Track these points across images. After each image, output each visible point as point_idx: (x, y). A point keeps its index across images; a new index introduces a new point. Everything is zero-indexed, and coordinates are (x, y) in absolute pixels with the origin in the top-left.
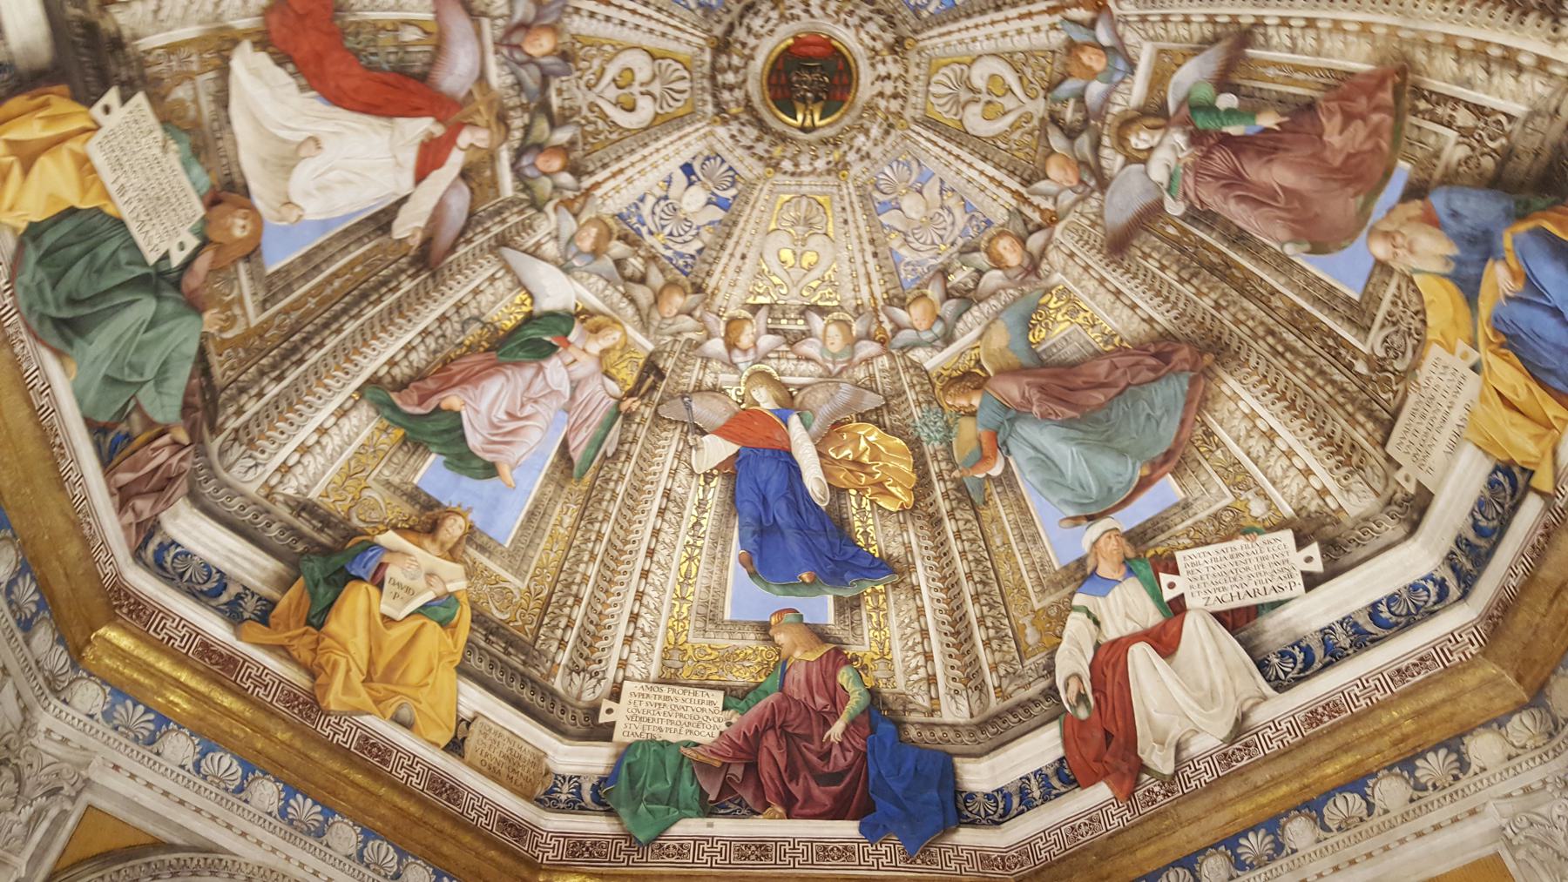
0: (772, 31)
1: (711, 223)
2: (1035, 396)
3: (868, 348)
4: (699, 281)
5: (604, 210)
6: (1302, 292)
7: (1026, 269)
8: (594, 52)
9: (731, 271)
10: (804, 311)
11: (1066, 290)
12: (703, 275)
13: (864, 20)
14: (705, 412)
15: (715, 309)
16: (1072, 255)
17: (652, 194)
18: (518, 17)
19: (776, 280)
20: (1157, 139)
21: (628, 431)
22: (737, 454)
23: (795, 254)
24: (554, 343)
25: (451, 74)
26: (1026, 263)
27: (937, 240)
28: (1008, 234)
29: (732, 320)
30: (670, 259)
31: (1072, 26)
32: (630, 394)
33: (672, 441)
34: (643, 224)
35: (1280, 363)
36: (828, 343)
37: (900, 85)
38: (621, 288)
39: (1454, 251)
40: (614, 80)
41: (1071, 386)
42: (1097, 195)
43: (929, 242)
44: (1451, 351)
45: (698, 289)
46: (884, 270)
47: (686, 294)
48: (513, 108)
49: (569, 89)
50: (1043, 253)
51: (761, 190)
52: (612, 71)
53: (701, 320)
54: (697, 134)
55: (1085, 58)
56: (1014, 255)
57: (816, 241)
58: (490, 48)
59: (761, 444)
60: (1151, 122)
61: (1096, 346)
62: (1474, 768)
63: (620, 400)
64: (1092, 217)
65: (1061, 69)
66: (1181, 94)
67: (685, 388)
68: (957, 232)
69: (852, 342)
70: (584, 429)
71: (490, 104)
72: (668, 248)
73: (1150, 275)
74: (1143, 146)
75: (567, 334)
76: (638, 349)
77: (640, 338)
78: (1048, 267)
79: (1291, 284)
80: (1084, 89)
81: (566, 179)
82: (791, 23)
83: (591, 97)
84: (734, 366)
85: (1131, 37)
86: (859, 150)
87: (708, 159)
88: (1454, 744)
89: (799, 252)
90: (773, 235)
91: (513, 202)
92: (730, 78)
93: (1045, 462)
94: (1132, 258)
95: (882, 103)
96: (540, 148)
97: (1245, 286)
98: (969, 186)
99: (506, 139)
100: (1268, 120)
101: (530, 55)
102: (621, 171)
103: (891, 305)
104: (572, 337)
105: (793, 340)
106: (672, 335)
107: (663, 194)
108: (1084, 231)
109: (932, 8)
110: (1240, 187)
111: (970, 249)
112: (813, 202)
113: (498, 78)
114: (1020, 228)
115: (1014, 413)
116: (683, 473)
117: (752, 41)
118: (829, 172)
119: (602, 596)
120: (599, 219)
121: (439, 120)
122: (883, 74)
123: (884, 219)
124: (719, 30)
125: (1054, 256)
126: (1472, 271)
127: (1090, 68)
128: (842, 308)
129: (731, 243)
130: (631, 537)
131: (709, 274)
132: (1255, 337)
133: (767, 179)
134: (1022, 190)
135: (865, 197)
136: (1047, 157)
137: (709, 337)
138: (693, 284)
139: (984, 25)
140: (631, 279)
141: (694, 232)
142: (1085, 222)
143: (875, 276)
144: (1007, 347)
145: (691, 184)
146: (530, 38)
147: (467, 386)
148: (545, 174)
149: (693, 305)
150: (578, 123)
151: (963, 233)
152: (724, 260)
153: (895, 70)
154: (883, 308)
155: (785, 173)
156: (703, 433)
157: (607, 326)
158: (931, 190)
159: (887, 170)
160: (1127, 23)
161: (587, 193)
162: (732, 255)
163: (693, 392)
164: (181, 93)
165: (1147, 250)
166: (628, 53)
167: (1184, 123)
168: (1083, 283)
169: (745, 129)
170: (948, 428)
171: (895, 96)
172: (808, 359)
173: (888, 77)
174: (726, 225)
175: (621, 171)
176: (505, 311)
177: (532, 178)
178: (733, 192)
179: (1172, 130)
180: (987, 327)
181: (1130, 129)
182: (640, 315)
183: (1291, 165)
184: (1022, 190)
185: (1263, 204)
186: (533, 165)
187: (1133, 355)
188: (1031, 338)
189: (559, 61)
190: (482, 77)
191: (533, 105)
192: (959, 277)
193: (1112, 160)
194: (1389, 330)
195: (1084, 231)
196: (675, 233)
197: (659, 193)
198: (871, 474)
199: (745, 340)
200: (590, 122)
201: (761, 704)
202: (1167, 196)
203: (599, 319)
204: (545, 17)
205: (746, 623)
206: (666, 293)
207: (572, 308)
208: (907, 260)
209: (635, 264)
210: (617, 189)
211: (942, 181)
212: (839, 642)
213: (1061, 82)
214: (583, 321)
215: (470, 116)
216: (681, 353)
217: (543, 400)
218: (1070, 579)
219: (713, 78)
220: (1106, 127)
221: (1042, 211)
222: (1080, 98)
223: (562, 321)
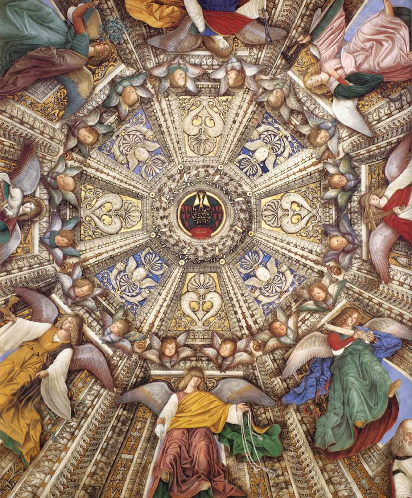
0: (222, 238)
1: (254, 140)
3: (160, 72)
4: (260, 109)
5: (311, 151)
7: (75, 128)
8: (311, 234)
9: (241, 113)
10: (198, 93)
11: (52, 120)
12: (257, 112)
13: (176, 245)
15: (250, 93)
16: (52, 138)
17: (285, 158)
18: (348, 257)
19: (215, 109)
20: (21, 209)
21: (307, 22)
23: (205, 124)
24: (347, 82)
25: (385, 236)
26: (76, 131)
27: (127, 137)
28: (88, 145)
29: (241, 87)
30: (276, 122)
31: (75, 254)
34: (290, 142)
36: (183, 75)
37: (155, 214)
38: (305, 108)
40: (302, 219)
41: (38, 69)
42: (46, 173)
43: (131, 136)
45: (260, 104)
46: (154, 118)
47: (267, 101)
48: (355, 212)
49: (326, 217)
50: (67, 137)
51: (225, 158)
52: (302, 224)
53: (259, 86)
54: (260, 187)
55: (65, 240)
56: (83, 134)
57: (195, 131)
58: (364, 244)
60: (26, 217)
61: (27, 93)
64: (45, 161)
65: (76, 233)
66: (15, 234)
67: (270, 46)
68: (117, 143)
69: (170, 75)
70: (334, 28)
71: (367, 218)
72: (278, 129)
73: (7, 136)
74: (28, 205)
75: (338, 86)
76: (297, 73)
77: (295, 78)
78: (63, 130)
80: (63, 226)
81: (331, 170)
82: (212, 242)
83: (314, 212)
84: (240, 60)
85: (45, 255)
86: (174, 180)
87: (254, 175)
89: (203, 125)
90: (218, 134)
91: (362, 161)
92: (242, 216)
94: (19, 143)
95: (164, 205)
96: (343, 189)
98: (113, 167)
99: (361, 197)
101: (343, 237)
102: (300, 171)
103: (149, 98)
105: (205, 76)
106: (276, 79)
107: (278, 158)
108: (48, 152)
109: (144, 253)
111: (109, 134)
112: (196, 151)
113: (362, 230)
114: (83, 149)
115: (69, 45)
117: (231, 234)
118: (189, 168)
120: (315, 147)
121: (396, 215)
122: (165, 220)
123: (157, 146)
124: (248, 240)
125: (62, 137)
127: (62, 237)
128: (177, 95)
129: (241, 129)
131: (254, 112)
133: (223, 163)
134: (84, 168)
135: (169, 156)
136: (75, 188)
137: (254, 76)
138: (263, 107)
139: (118, 248)
140: (299, 113)
141: (263, 136)
142: (49, 158)
143: (159, 114)
144: (78, 84)
145: (264, 162)
146: (343, 245)
147: (403, 64)
148: (343, 174)
149: (263, 95)
150: (322, 199)
151: (113, 143)
152: (245, 120)
153: (159, 222)
154: (153, 96)
155: (212, 167)
157: (314, 87)
158: (133, 163)
159: (158, 171)
160: (49, 261)
161: (320, 160)
162: (241, 123)
163: (265, 44)
165: (11, 150)
166: (294, 232)
167: (10, 220)
168: (42, 125)
169: (234, 189)
171: (157, 209)
172: (195, 65)
173: (162, 218)
174: (244, 139)
175: (300, 171)
177: (349, 173)
178: (240, 157)
179: (14, 216)
180: (91, 93)
181: (36, 211)
182: (295, 92)
184: (84, 168)
186: (348, 181)
187: (5, 92)
188: (65, 91)
189: (329, 232)
190: (369, 232)
191: (345, 212)
192: (111, 119)
193: (41, 194)
195: (48, 152)
196: (272, 136)
197: (281, 159)
199: (233, 75)
200: (317, 198)
202: (9, 182)
203: (319, 92)
204: (335, 254)
206: (279, 103)
207: (335, 100)
208: (142, 125)
209: (296, 121)
210: (304, 161)
211: (128, 168)
213: (75, 226)
214: (329, 92)
215: (379, 213)
216: (271, 67)
217: (358, 49)
219: (251, 216)
220: (48, 210)
221: (72, 159)
222: (64, 222)
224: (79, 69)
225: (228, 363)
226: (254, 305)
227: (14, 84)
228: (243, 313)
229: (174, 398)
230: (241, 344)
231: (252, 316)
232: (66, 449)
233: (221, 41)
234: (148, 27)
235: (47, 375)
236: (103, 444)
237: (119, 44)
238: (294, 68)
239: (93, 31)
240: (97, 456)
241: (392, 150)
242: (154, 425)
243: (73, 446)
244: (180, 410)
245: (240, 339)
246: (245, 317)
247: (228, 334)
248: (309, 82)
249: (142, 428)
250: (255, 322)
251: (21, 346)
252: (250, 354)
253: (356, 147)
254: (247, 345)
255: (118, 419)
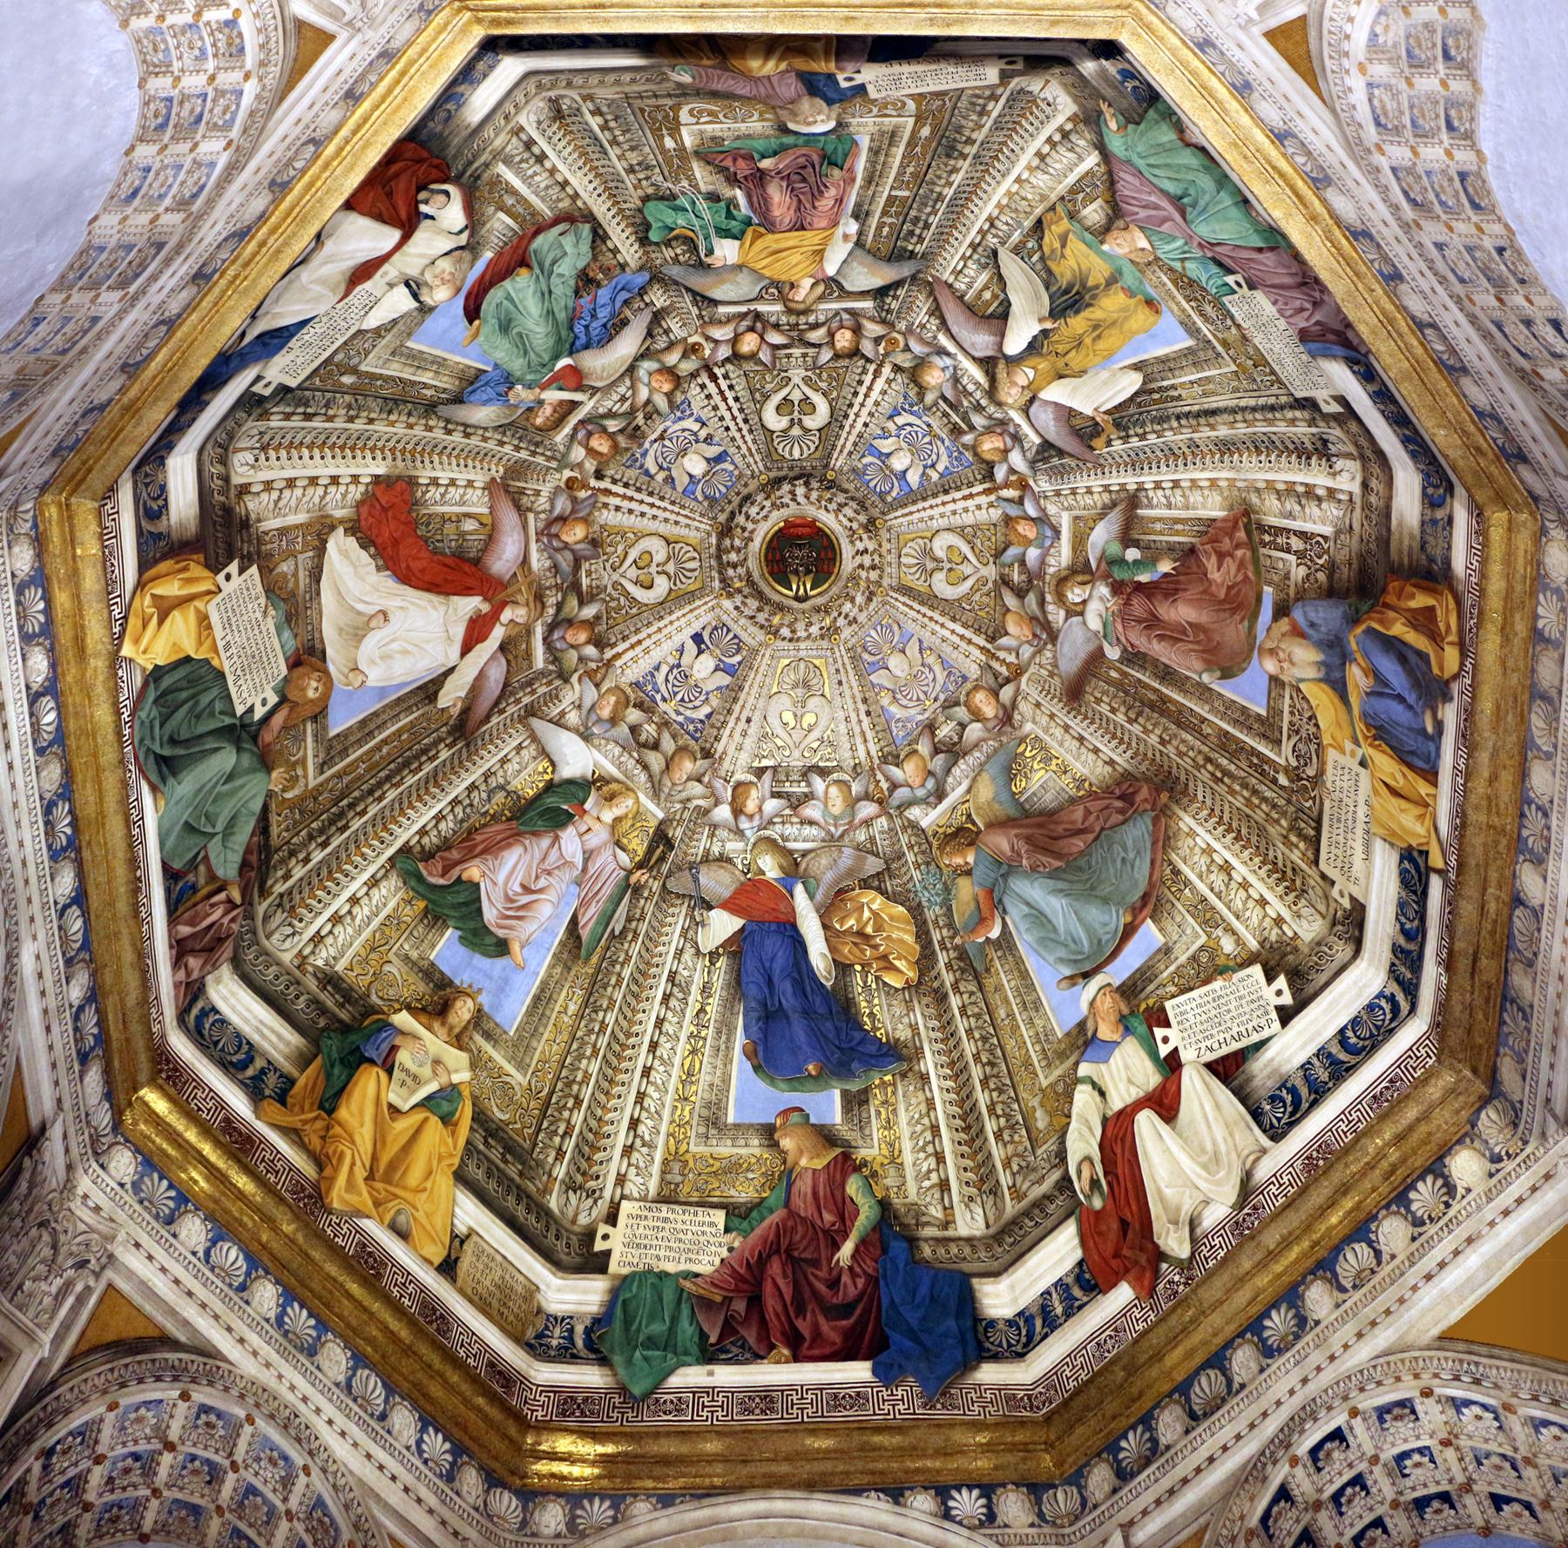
2: (1023, 847)
6: (1223, 716)
14: (712, 884)
22: (742, 930)
32: (640, 866)
33: (678, 917)
35: (1221, 789)
39: (1320, 657)
44: (1343, 752)
59: (767, 917)
62: (1460, 1191)
63: (630, 873)
77: (650, 805)
79: (1212, 710)
88: (1436, 1168)
93: (1039, 918)
97: (1181, 719)
100: (1165, 567)
104: (587, 806)
110: (1157, 627)
115: (1006, 868)
116: (687, 956)
119: (602, 1098)
126: (1337, 675)
130: (636, 1028)
132: (1197, 767)
156: (710, 908)
164: (285, 567)
170: (947, 890)
176: (526, 778)
183: (1190, 602)
185: (1177, 640)
194: (1294, 739)
198: (876, 947)
201: (766, 1224)
203: (614, 786)
205: (751, 1126)
212: (847, 1145)
218: (1073, 1047)
223: (580, 788)
224: (990, 825)
225: (745, 323)
226: (706, 414)
227: (1088, 812)
228: (725, 399)
229: (831, 270)
230: (724, 352)
231: (709, 397)
232: (998, 205)
233: (770, 867)
234: (883, 892)
235: (1041, 320)
236: (942, 207)
237: (928, 864)
238: (653, 823)
239: (966, 890)
240: (949, 193)
241: (497, 703)
242: (860, 233)
243: (989, 209)
244: (819, 254)
245: (727, 360)
246: (721, 393)
247: (749, 366)
248: (630, 802)
249: (880, 226)
250: (703, 387)
251: (1084, 372)
252: (708, 338)
253: (554, 697)
254: (714, 351)
255: (921, 239)
